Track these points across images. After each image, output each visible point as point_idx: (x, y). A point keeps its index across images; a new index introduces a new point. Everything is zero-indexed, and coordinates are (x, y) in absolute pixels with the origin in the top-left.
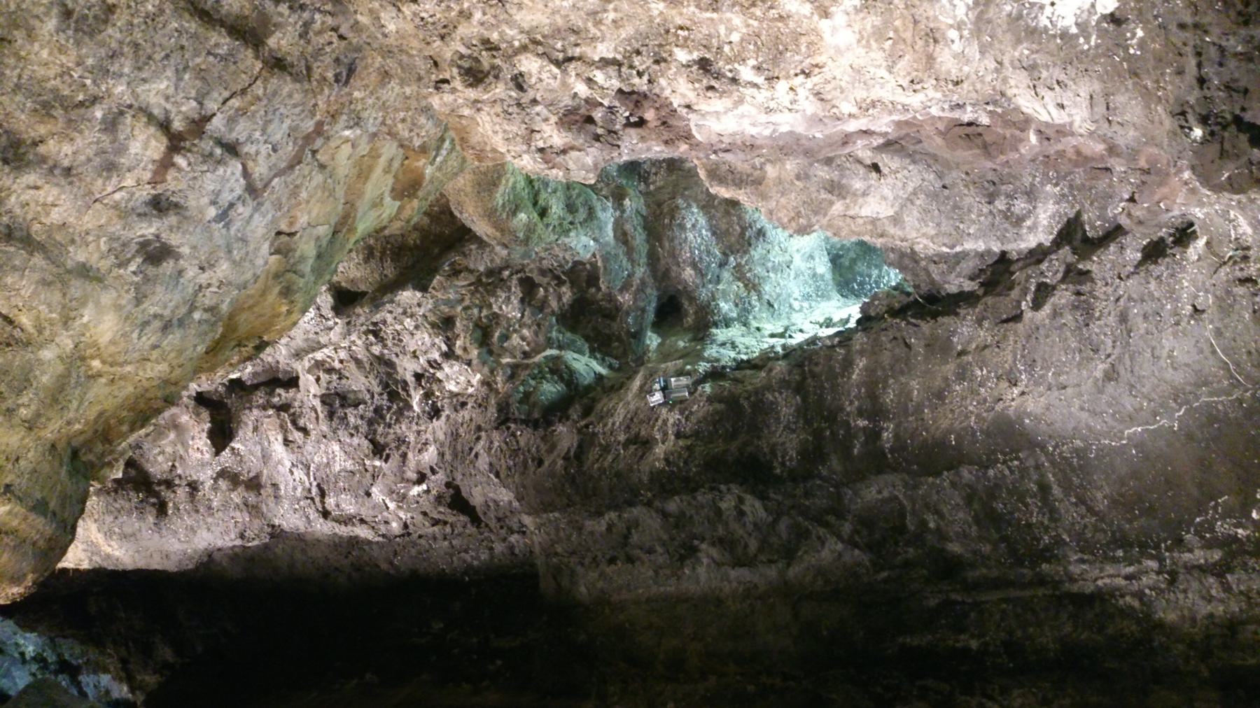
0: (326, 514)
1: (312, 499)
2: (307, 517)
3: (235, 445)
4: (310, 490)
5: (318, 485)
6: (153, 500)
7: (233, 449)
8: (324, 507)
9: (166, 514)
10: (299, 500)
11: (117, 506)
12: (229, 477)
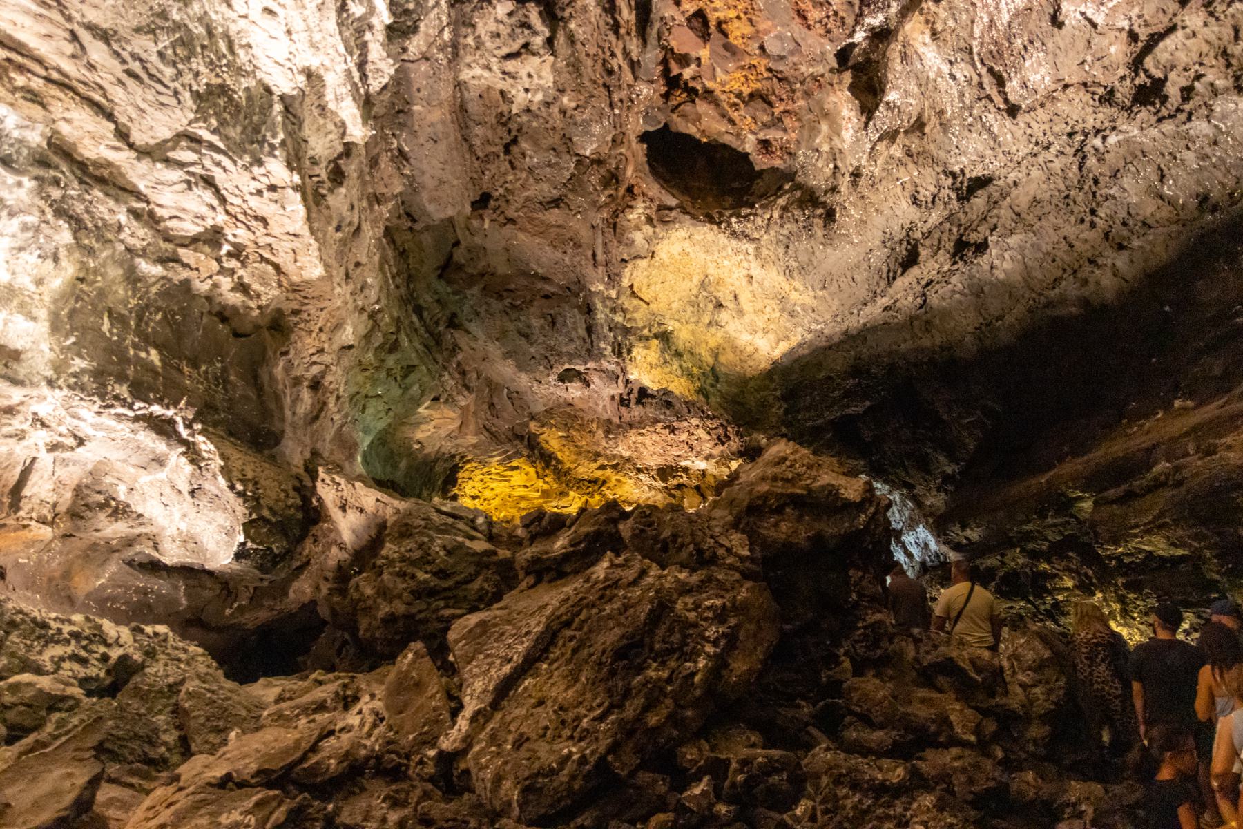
0: (1013, 111)
1: (989, 97)
2: (990, 131)
3: (892, 96)
4: (980, 85)
5: (991, 70)
6: (819, 211)
7: (888, 103)
8: (1006, 101)
9: (834, 221)
10: (972, 107)
11: (785, 232)
12: (891, 136)
